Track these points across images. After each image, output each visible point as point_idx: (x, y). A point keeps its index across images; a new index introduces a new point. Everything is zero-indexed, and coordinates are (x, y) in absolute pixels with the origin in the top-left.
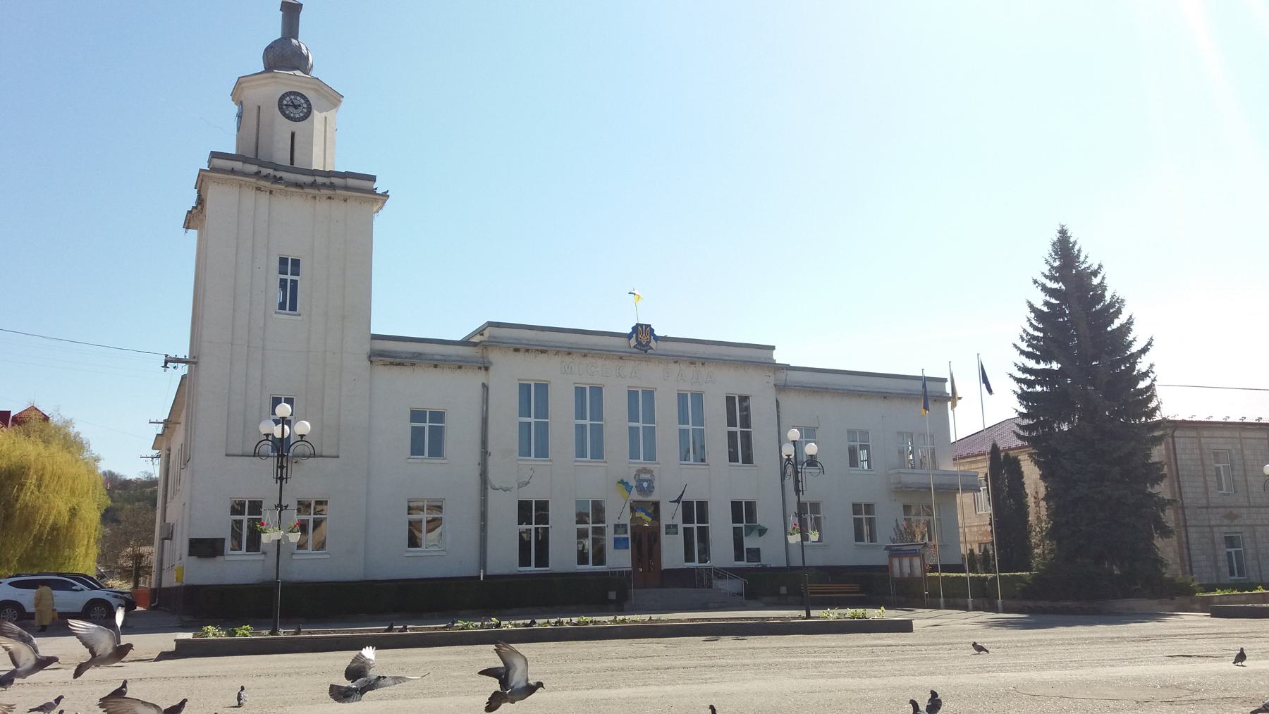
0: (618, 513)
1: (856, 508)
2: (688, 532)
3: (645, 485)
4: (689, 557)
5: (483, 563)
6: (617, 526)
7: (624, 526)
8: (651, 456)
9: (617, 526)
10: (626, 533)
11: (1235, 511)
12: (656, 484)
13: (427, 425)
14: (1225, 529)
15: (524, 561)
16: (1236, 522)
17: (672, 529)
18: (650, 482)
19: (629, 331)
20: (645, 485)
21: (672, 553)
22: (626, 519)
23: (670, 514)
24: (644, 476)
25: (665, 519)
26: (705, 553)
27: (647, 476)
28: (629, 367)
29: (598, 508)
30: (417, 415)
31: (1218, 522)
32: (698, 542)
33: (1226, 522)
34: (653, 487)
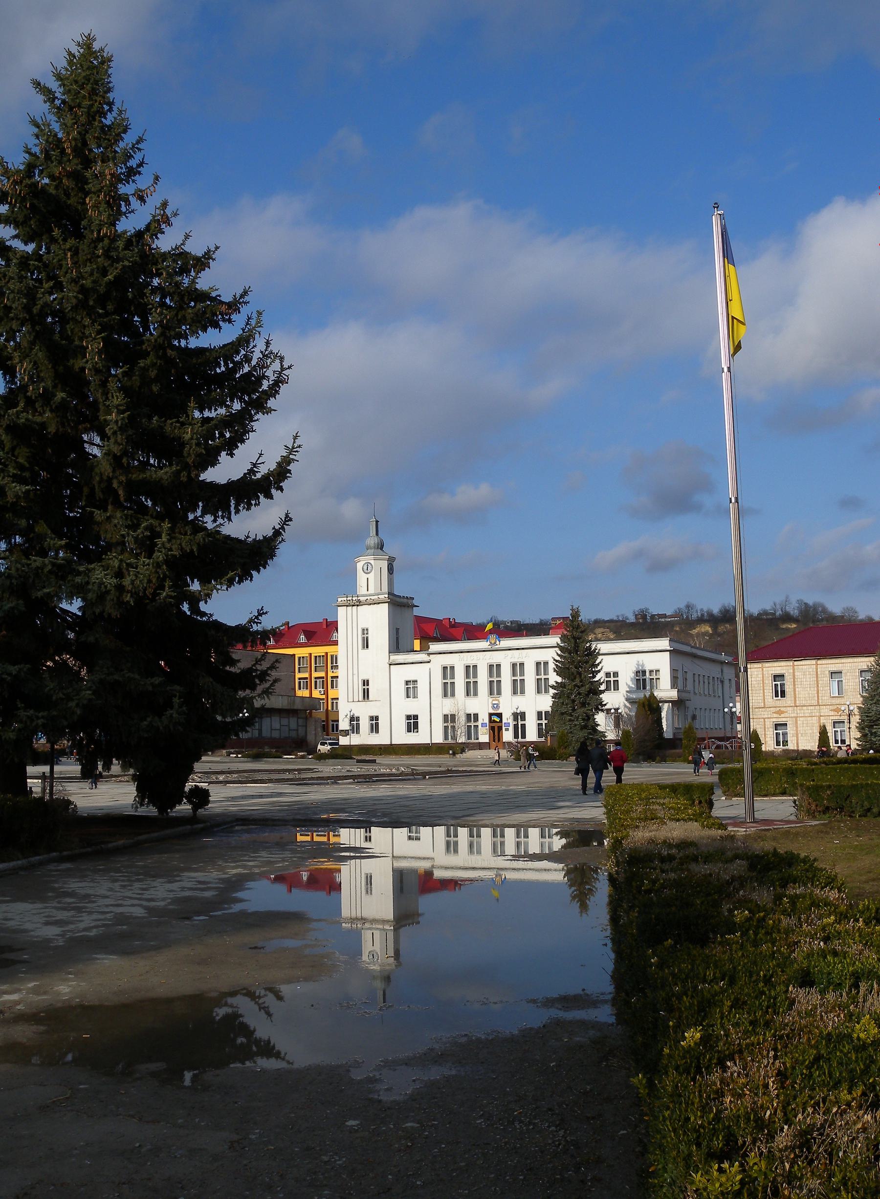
0: (484, 718)
2: (516, 727)
4: (516, 736)
5: (391, 742)
8: (499, 693)
11: (782, 709)
14: (774, 720)
15: (446, 738)
16: (782, 715)
17: (508, 724)
21: (508, 736)
22: (487, 721)
23: (507, 718)
24: (494, 702)
25: (504, 721)
26: (524, 736)
27: (496, 702)
29: (476, 716)
30: (407, 682)
31: (769, 716)
32: (520, 730)
33: (775, 715)
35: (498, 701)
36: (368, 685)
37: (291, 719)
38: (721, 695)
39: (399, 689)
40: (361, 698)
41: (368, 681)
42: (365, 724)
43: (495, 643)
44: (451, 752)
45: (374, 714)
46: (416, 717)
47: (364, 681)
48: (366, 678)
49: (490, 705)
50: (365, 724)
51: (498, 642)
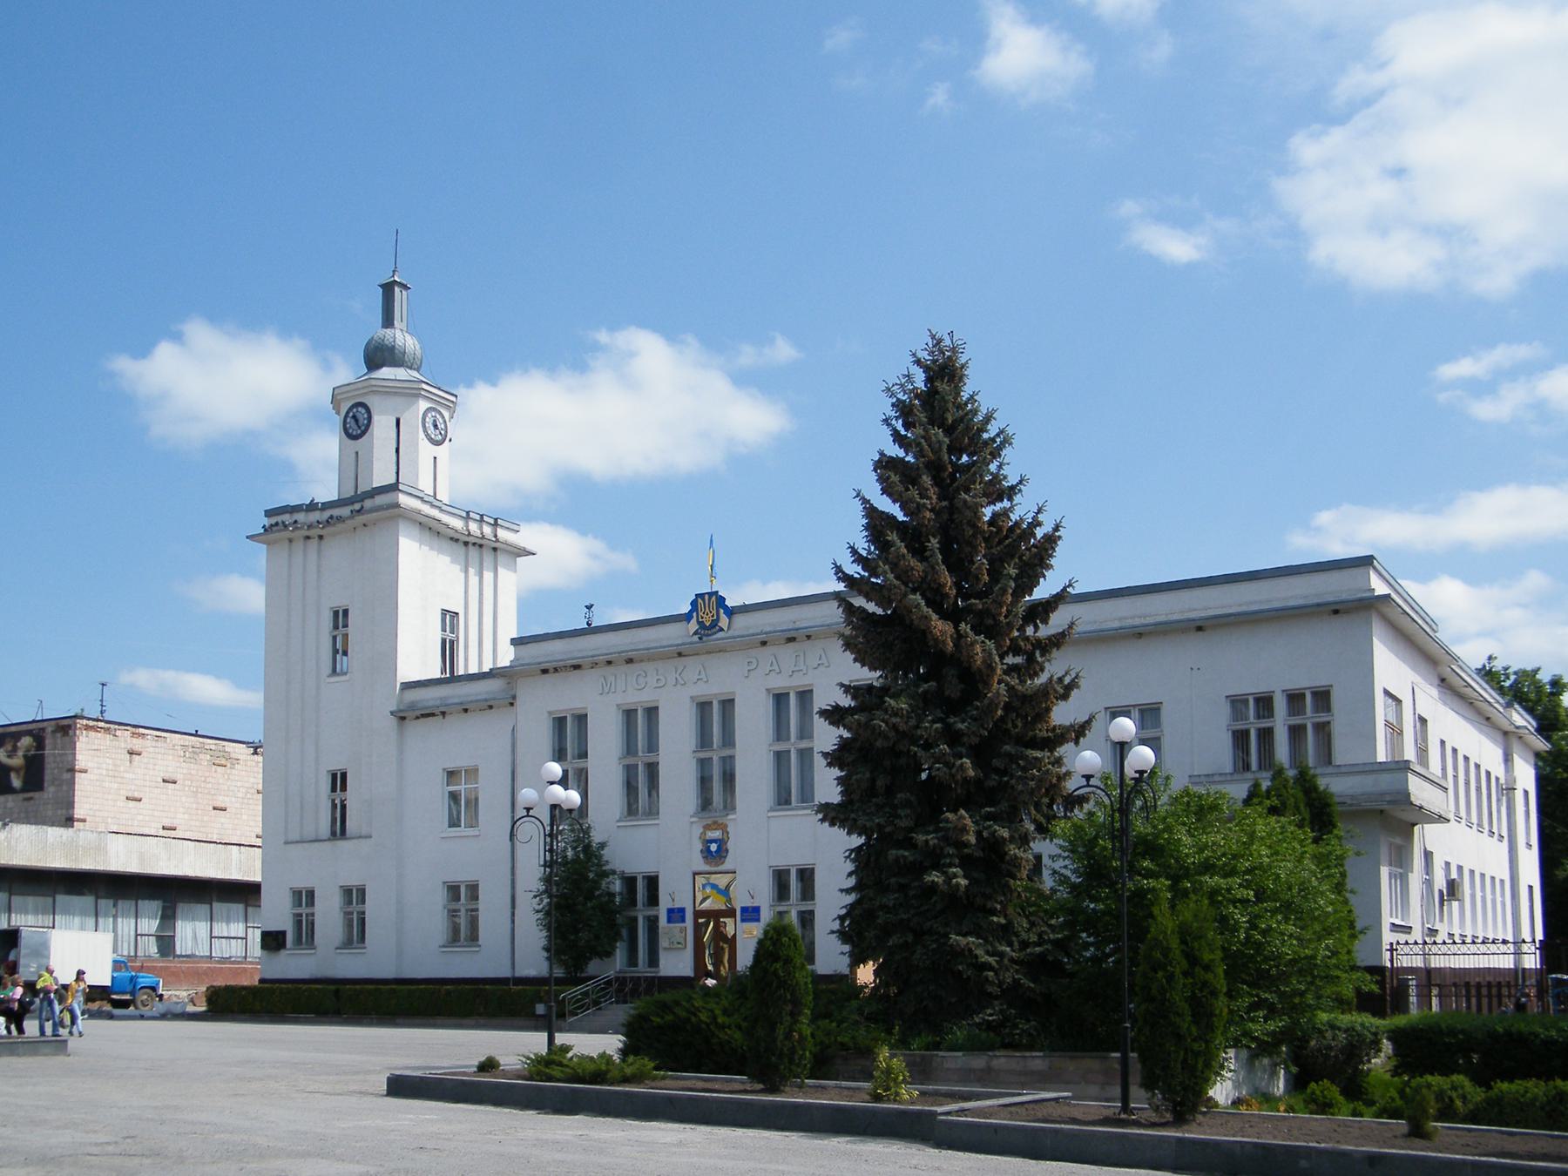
1: (453, 890)
3: (714, 847)
6: (670, 911)
7: (682, 910)
9: (670, 911)
10: (683, 920)
12: (730, 845)
13: (464, 786)
18: (721, 843)
19: (685, 608)
20: (714, 847)
24: (712, 835)
27: (717, 834)
28: (692, 667)
34: (727, 851)
35: (724, 828)
36: (344, 788)
37: (215, 905)
38: (1505, 833)
39: (430, 797)
40: (324, 827)
41: (344, 775)
42: (329, 916)
43: (715, 623)
44: (540, 1009)
45: (353, 881)
46: (473, 889)
47: (334, 776)
48: (337, 766)
49: (699, 846)
50: (329, 916)
51: (724, 621)
